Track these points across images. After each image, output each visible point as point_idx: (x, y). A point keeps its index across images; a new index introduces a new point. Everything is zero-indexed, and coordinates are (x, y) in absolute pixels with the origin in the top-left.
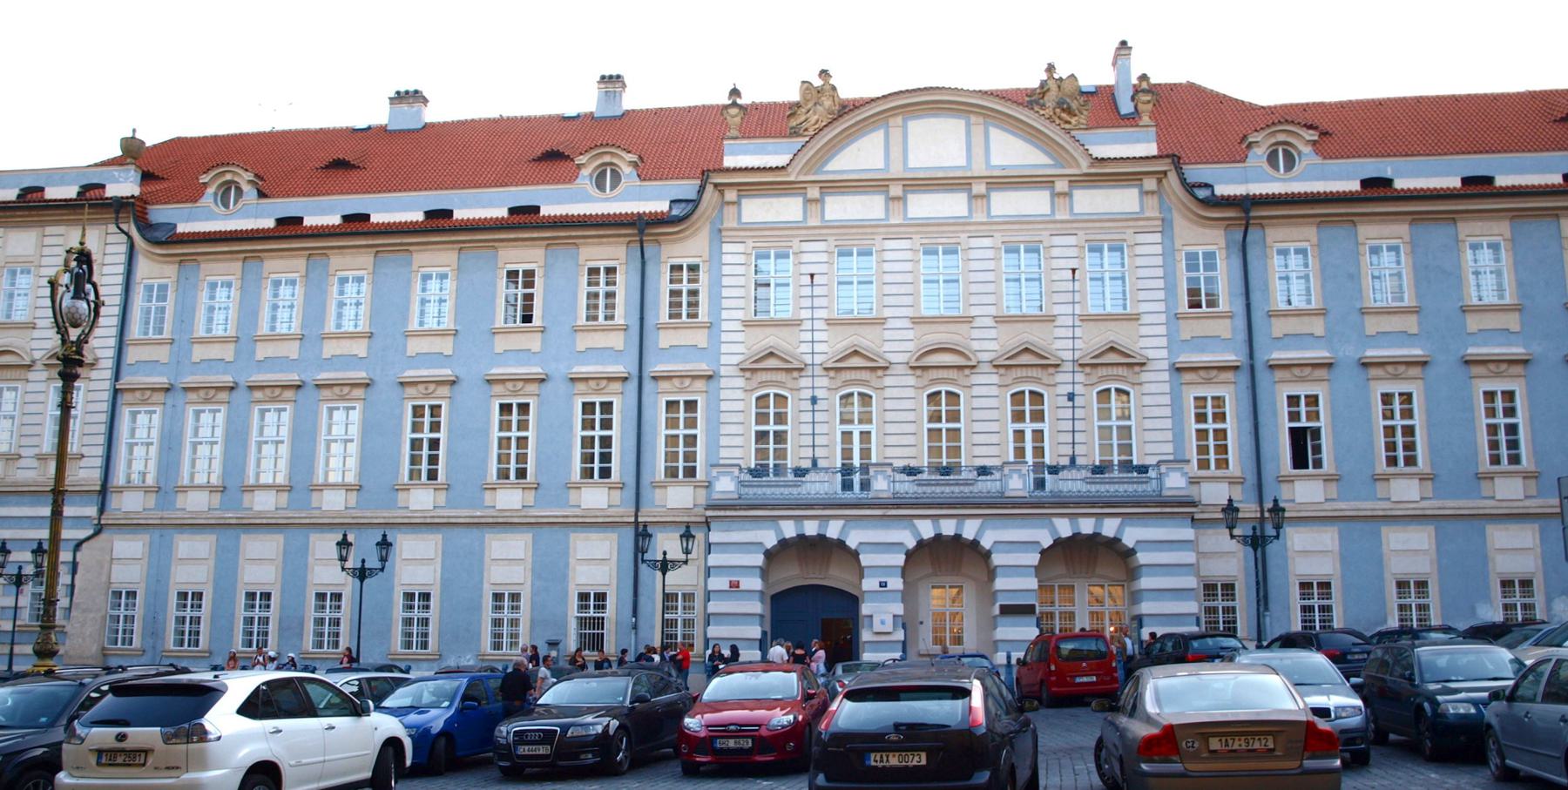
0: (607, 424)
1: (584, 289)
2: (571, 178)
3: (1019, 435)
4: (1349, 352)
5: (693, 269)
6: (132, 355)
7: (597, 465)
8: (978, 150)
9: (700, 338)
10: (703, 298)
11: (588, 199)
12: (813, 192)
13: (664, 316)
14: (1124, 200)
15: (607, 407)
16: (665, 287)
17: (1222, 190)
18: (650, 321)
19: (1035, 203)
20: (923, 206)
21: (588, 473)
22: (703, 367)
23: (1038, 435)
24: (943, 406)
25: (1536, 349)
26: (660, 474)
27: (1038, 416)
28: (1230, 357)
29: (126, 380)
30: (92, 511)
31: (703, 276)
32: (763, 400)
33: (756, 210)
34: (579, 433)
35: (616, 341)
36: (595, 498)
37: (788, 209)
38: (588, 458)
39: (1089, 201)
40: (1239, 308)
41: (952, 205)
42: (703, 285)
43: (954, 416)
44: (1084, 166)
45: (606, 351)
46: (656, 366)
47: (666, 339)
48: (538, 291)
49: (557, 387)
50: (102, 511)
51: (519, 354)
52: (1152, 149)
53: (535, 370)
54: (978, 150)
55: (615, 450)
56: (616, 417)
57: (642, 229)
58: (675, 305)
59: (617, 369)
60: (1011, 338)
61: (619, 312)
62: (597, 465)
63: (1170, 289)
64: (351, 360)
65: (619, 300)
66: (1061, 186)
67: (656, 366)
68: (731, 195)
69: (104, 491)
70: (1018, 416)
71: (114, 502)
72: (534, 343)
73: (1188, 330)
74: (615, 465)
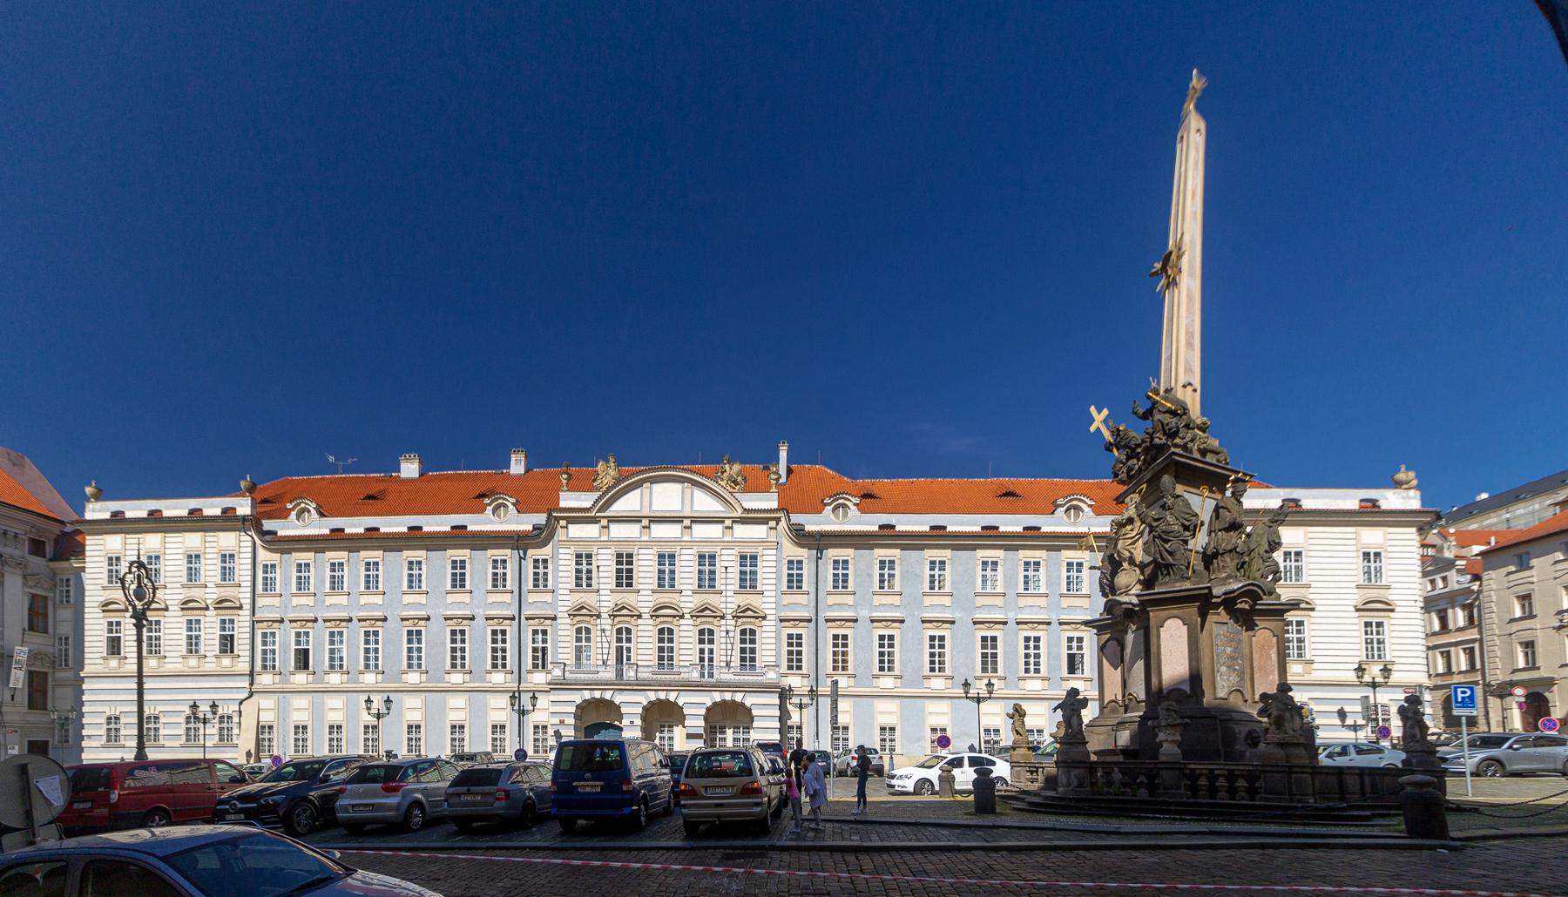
0: (504, 641)
1: (490, 571)
2: (482, 510)
3: (702, 651)
4: (864, 614)
5: (545, 561)
6: (260, 602)
7: (498, 662)
8: (687, 502)
9: (548, 597)
10: (550, 577)
11: (492, 522)
12: (604, 522)
13: (531, 587)
14: (759, 531)
15: (504, 632)
16: (531, 570)
17: (807, 528)
18: (524, 589)
19: (714, 531)
20: (659, 531)
21: (495, 666)
22: (550, 613)
23: (711, 651)
24: (665, 635)
25: (957, 615)
26: (530, 667)
27: (711, 641)
28: (805, 614)
29: (258, 615)
30: (247, 684)
31: (550, 565)
32: (579, 631)
33: (576, 531)
34: (490, 645)
35: (507, 598)
36: (498, 678)
37: (591, 531)
38: (494, 658)
39: (742, 531)
40: (812, 591)
41: (674, 531)
42: (550, 571)
43: (671, 640)
44: (739, 513)
45: (504, 603)
46: (526, 612)
47: (532, 598)
48: (468, 571)
49: (480, 621)
50: (252, 684)
51: (459, 603)
52: (774, 505)
53: (467, 613)
54: (687, 502)
55: (508, 654)
56: (508, 637)
57: (519, 542)
58: (536, 580)
59: (508, 613)
60: (699, 600)
61: (508, 583)
62: (498, 662)
63: (779, 579)
64: (374, 606)
65: (508, 577)
66: (728, 523)
67: (526, 612)
68: (563, 523)
69: (252, 674)
70: (701, 641)
71: (258, 679)
72: (466, 598)
73: (788, 599)
74: (508, 662)
